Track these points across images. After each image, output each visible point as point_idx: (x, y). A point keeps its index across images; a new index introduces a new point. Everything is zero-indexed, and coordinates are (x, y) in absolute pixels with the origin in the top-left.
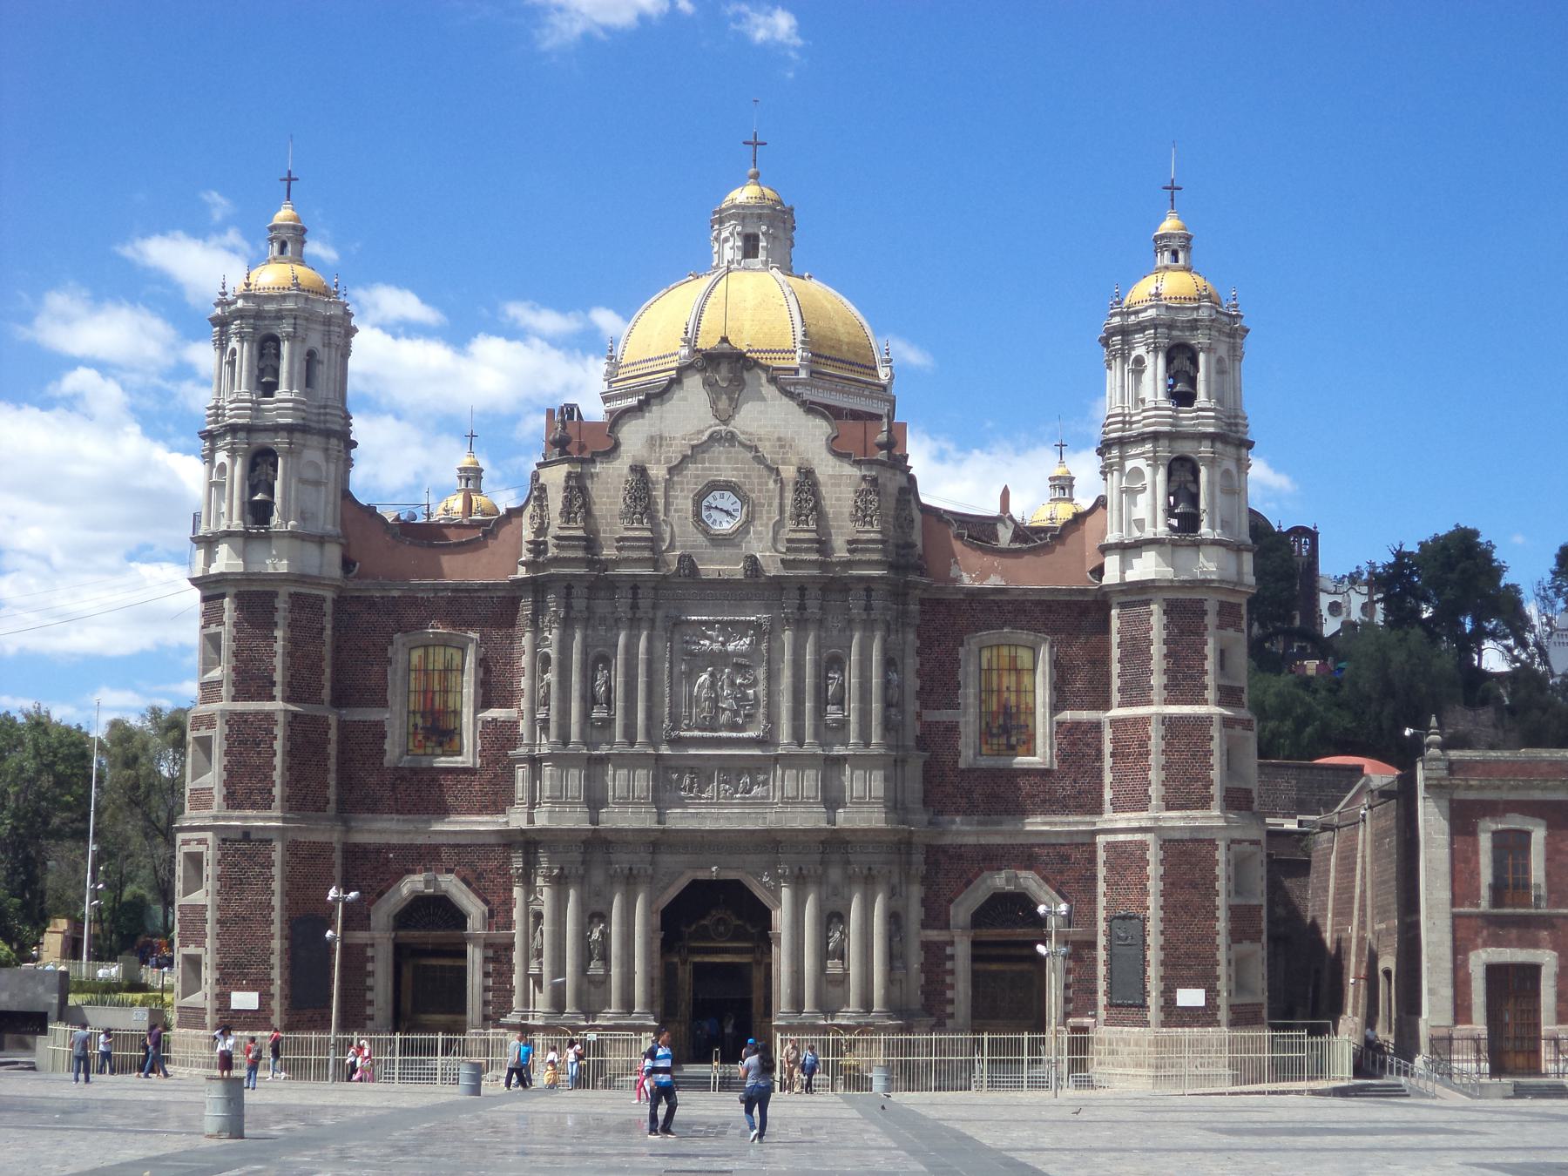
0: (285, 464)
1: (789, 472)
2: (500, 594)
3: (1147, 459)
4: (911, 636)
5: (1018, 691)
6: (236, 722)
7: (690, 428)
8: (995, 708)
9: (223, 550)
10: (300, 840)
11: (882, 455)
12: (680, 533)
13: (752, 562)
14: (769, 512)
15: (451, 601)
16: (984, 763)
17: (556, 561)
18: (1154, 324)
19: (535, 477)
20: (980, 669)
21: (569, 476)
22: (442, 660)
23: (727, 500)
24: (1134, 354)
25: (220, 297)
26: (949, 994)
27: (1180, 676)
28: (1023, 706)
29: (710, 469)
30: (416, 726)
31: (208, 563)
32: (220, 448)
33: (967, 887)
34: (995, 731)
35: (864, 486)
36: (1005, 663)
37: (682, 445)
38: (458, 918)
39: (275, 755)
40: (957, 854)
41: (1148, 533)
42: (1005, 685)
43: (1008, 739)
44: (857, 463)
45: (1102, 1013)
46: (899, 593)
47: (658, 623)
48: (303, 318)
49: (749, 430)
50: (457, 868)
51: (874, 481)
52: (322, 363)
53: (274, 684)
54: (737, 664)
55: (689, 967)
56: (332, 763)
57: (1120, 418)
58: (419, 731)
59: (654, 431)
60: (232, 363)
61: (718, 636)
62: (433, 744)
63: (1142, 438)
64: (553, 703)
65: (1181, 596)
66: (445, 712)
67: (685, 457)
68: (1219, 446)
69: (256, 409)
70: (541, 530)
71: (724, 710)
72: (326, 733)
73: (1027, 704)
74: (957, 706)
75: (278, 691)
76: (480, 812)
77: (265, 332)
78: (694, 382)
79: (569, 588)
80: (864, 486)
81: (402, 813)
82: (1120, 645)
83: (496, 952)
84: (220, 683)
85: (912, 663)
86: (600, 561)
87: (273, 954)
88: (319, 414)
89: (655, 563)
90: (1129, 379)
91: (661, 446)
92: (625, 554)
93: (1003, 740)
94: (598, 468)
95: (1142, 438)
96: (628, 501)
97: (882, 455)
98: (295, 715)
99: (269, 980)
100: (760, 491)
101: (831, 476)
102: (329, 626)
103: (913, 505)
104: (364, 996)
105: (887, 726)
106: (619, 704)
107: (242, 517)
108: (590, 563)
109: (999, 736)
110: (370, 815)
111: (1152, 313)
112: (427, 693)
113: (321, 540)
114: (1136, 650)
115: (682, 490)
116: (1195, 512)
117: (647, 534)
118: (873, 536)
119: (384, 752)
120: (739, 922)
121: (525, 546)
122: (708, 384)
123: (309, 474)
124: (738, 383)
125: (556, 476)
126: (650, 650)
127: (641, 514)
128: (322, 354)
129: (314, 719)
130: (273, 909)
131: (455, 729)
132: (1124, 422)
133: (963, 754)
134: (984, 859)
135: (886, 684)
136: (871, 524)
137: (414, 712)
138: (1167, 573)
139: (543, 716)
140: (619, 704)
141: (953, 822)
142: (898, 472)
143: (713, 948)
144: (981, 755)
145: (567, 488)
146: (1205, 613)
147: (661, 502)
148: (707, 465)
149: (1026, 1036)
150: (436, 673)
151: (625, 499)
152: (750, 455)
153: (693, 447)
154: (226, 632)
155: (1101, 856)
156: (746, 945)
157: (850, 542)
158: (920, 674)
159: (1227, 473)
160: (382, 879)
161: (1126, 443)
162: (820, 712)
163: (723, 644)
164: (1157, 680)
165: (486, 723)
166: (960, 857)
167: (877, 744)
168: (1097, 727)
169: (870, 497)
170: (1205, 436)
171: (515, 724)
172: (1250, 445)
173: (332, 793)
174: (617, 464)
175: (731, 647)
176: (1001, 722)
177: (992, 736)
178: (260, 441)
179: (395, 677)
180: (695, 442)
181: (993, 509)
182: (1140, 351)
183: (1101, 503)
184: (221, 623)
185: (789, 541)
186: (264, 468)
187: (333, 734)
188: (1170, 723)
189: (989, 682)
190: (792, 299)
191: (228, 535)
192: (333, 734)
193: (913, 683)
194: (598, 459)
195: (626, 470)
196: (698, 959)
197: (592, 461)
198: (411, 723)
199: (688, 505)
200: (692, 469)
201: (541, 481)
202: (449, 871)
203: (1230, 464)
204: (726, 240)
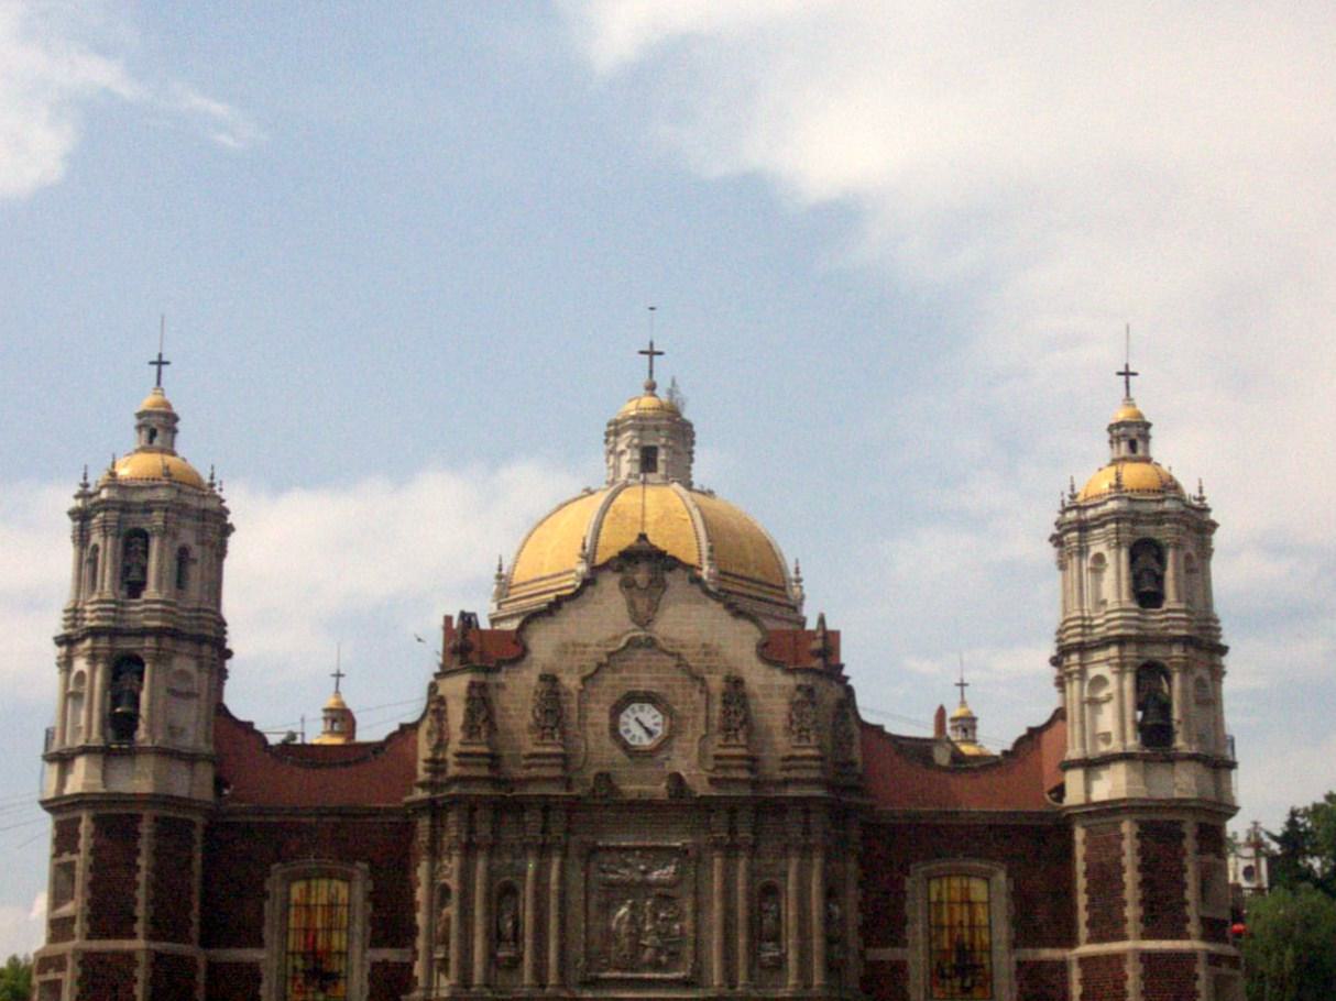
0: (153, 672)
1: (716, 683)
2: (394, 819)
3: (1111, 665)
4: (852, 866)
5: (972, 927)
6: (89, 961)
7: (607, 632)
8: (946, 945)
9: (81, 764)
11: (817, 663)
12: (597, 749)
13: (677, 779)
17: (456, 780)
18: (1117, 517)
19: (433, 688)
20: (929, 903)
21: (472, 685)
22: (325, 894)
23: (650, 716)
24: (1094, 550)
25: (80, 489)
28: (977, 943)
29: (631, 679)
30: (295, 968)
31: (62, 782)
32: (78, 655)
34: (947, 971)
35: (799, 696)
36: (957, 896)
37: (596, 653)
41: (1115, 746)
42: (957, 917)
43: (963, 981)
44: (790, 671)
46: (839, 814)
47: (572, 851)
48: (176, 510)
49: (672, 635)
51: (810, 691)
52: (194, 561)
53: (135, 919)
54: (660, 895)
57: (1079, 622)
60: (93, 561)
61: (638, 865)
63: (1105, 643)
64: (453, 941)
65: (1154, 816)
66: (328, 952)
67: (600, 666)
68: (1191, 651)
69: (119, 608)
70: (441, 745)
71: (645, 947)
72: (193, 977)
73: (982, 941)
74: (905, 944)
75: (139, 927)
77: (136, 525)
78: (610, 582)
79: (473, 809)
80: (799, 696)
82: (1086, 874)
84: (72, 920)
85: (853, 895)
86: (506, 782)
88: (190, 618)
89: (568, 783)
90: (1088, 578)
93: (957, 982)
94: (501, 678)
95: (1105, 643)
96: (538, 714)
97: (817, 663)
101: (761, 687)
102: (198, 855)
103: (852, 719)
105: (833, 968)
106: (528, 941)
107: (103, 733)
108: (495, 782)
111: (1112, 505)
112: (309, 931)
113: (192, 759)
114: (1105, 879)
116: (1166, 723)
117: (560, 750)
118: (810, 752)
121: (421, 765)
122: (628, 585)
123: (182, 687)
124: (657, 584)
125: (457, 686)
126: (562, 879)
128: (196, 552)
129: (180, 959)
131: (340, 971)
132: (1083, 626)
135: (828, 919)
136: (808, 738)
137: (293, 953)
138: (1141, 792)
139: (441, 955)
140: (528, 941)
142: (834, 683)
145: (470, 699)
146: (1183, 836)
147: (574, 717)
150: (319, 909)
151: (534, 712)
152: (672, 662)
153: (611, 654)
154: (81, 859)
157: (784, 759)
158: (861, 907)
159: (1200, 683)
161: (1086, 649)
162: (753, 952)
163: (645, 873)
164: (1131, 912)
165: (375, 965)
167: (819, 985)
168: (1063, 966)
169: (806, 710)
170: (1175, 640)
171: (411, 966)
172: (1223, 650)
174: (525, 673)
175: (655, 876)
176: (954, 961)
177: (943, 976)
178: (125, 646)
179: (271, 909)
180: (611, 649)
181: (929, 733)
182: (1098, 547)
183: (1060, 715)
184: (75, 850)
185: (717, 757)
186: (127, 681)
187: (201, 978)
188: (1147, 958)
189: (939, 915)
190: (696, 513)
191: (85, 750)
193: (855, 918)
195: (534, 679)
197: (497, 669)
198: (290, 965)
199: (605, 719)
200: (609, 679)
201: (441, 692)
203: (1202, 672)
204: (622, 452)
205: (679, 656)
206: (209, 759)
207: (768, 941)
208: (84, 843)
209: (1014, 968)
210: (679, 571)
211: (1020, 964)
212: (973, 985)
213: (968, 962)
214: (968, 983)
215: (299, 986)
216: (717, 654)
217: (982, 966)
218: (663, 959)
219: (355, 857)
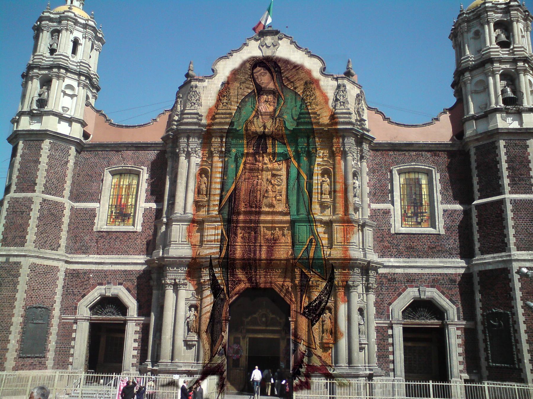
10: (37, 263)
16: (404, 230)
24: (473, 30)
26: (391, 357)
27: (516, 179)
30: (112, 212)
33: (399, 297)
38: (122, 308)
39: (30, 218)
40: (392, 279)
41: (493, 106)
43: (417, 219)
45: (485, 372)
50: (124, 282)
52: (81, 44)
56: (65, 227)
58: (114, 214)
75: (36, 188)
81: (99, 254)
82: (477, 168)
87: (12, 325)
88: (77, 66)
92: (217, 121)
94: (205, 84)
98: (44, 200)
99: (7, 340)
104: (69, 351)
109: (411, 217)
113: (70, 121)
118: (344, 111)
119: (93, 224)
127: (227, 103)
128: (82, 41)
129: (56, 203)
130: (16, 300)
133: (393, 226)
134: (408, 281)
143: (259, 330)
144: (402, 227)
149: (431, 383)
155: (476, 279)
156: (277, 328)
160: (86, 288)
165: (146, 209)
166: (395, 280)
173: (63, 242)
177: (409, 217)
188: (514, 202)
192: (67, 212)
193: (367, 190)
194: (207, 80)
196: (251, 336)
202: (120, 284)
206: (78, 121)
207: (325, 194)
208: (20, 152)
210: (284, 39)
211: (445, 211)
212: (422, 220)
214: (419, 220)
218: (275, 202)
219: (143, 164)
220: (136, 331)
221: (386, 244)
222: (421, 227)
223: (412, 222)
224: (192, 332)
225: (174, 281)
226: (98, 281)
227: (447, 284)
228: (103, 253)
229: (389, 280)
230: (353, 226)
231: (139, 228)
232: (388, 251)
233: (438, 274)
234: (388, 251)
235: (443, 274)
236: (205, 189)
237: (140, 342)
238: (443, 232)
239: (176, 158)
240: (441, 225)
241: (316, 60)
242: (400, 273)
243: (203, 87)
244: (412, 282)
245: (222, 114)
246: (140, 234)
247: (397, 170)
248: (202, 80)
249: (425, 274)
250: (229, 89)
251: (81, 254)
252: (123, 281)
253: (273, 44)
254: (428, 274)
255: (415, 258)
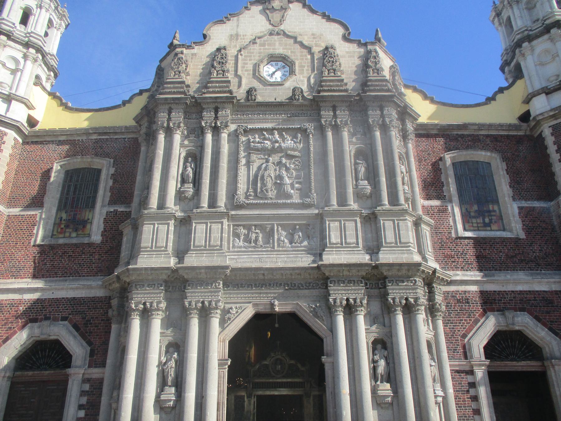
2: (129, 136)
14: (307, 70)
15: (97, 141)
34: (472, 214)
55: (254, 400)
58: (63, 222)
59: (234, 32)
62: (71, 230)
76: (95, 274)
83: (91, 386)
91: (237, 39)
93: (480, 220)
100: (303, 59)
101: (347, 52)
110: (13, 280)
115: (250, 60)
120: (292, 362)
131: (89, 219)
141: (458, 275)
148: (267, 47)
153: (259, 38)
176: (475, 207)
194: (196, 47)
196: (260, 393)
198: (58, 216)
202: (64, 319)
205: (295, 38)
209: (516, 211)
211: (520, 208)
212: (491, 220)
213: (485, 209)
214: (487, 220)
215: (62, 229)
216: (321, 38)
217: (494, 211)
220: (83, 391)
221: (447, 252)
222: (491, 230)
223: (477, 223)
224: (170, 386)
225: (142, 306)
226: (30, 316)
227: (540, 306)
228: (42, 275)
229: (459, 301)
230: (406, 220)
231: (96, 237)
232: (453, 262)
233: (526, 291)
234: (453, 262)
235: (533, 291)
236: (191, 175)
237: (88, 409)
238: (522, 235)
239: (151, 137)
240: (519, 227)
241: (337, 26)
242: (473, 291)
243: (192, 54)
244: (491, 303)
245: (217, 82)
246: (99, 246)
247: (450, 157)
248: (191, 46)
249: (509, 291)
250: (226, 55)
251: (9, 278)
252: (70, 314)
253: (282, 7)
254: (513, 291)
255: (490, 270)
